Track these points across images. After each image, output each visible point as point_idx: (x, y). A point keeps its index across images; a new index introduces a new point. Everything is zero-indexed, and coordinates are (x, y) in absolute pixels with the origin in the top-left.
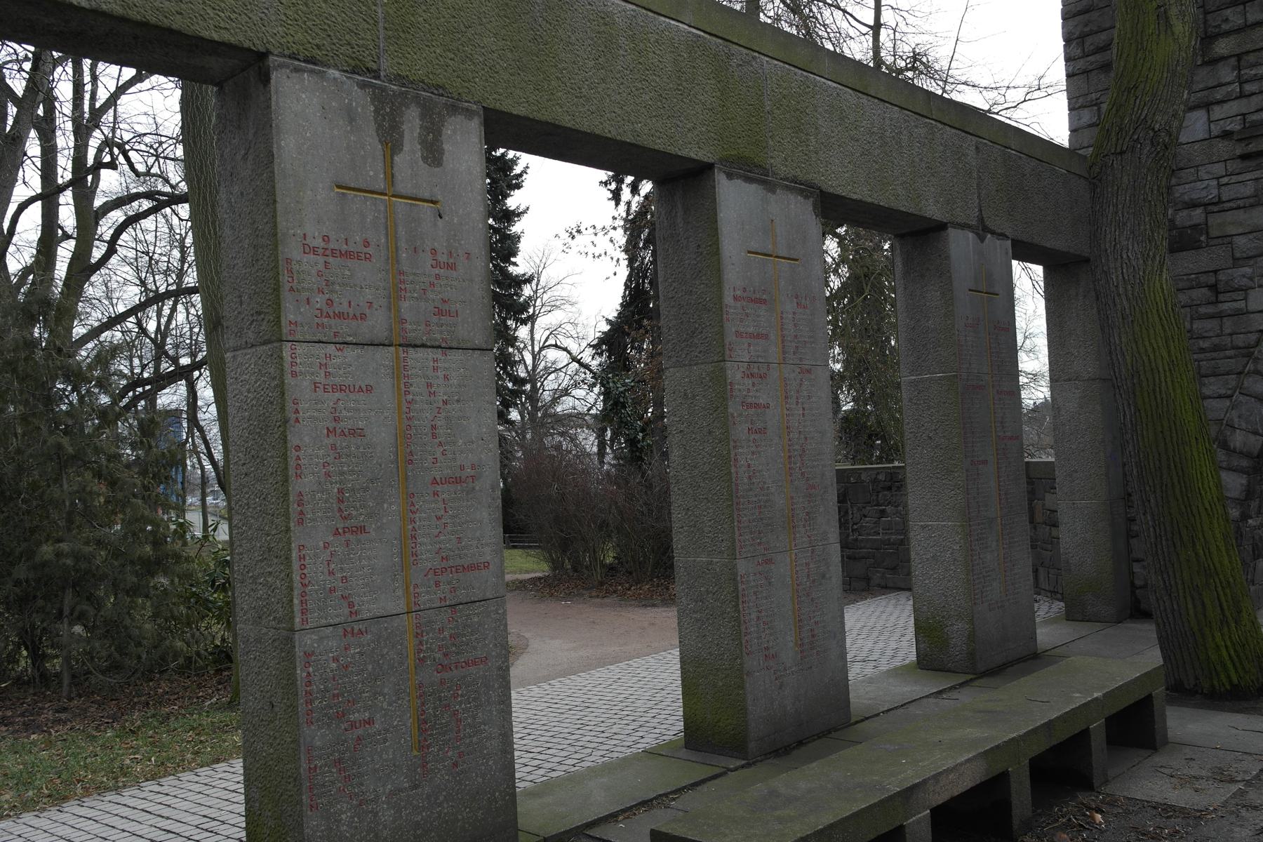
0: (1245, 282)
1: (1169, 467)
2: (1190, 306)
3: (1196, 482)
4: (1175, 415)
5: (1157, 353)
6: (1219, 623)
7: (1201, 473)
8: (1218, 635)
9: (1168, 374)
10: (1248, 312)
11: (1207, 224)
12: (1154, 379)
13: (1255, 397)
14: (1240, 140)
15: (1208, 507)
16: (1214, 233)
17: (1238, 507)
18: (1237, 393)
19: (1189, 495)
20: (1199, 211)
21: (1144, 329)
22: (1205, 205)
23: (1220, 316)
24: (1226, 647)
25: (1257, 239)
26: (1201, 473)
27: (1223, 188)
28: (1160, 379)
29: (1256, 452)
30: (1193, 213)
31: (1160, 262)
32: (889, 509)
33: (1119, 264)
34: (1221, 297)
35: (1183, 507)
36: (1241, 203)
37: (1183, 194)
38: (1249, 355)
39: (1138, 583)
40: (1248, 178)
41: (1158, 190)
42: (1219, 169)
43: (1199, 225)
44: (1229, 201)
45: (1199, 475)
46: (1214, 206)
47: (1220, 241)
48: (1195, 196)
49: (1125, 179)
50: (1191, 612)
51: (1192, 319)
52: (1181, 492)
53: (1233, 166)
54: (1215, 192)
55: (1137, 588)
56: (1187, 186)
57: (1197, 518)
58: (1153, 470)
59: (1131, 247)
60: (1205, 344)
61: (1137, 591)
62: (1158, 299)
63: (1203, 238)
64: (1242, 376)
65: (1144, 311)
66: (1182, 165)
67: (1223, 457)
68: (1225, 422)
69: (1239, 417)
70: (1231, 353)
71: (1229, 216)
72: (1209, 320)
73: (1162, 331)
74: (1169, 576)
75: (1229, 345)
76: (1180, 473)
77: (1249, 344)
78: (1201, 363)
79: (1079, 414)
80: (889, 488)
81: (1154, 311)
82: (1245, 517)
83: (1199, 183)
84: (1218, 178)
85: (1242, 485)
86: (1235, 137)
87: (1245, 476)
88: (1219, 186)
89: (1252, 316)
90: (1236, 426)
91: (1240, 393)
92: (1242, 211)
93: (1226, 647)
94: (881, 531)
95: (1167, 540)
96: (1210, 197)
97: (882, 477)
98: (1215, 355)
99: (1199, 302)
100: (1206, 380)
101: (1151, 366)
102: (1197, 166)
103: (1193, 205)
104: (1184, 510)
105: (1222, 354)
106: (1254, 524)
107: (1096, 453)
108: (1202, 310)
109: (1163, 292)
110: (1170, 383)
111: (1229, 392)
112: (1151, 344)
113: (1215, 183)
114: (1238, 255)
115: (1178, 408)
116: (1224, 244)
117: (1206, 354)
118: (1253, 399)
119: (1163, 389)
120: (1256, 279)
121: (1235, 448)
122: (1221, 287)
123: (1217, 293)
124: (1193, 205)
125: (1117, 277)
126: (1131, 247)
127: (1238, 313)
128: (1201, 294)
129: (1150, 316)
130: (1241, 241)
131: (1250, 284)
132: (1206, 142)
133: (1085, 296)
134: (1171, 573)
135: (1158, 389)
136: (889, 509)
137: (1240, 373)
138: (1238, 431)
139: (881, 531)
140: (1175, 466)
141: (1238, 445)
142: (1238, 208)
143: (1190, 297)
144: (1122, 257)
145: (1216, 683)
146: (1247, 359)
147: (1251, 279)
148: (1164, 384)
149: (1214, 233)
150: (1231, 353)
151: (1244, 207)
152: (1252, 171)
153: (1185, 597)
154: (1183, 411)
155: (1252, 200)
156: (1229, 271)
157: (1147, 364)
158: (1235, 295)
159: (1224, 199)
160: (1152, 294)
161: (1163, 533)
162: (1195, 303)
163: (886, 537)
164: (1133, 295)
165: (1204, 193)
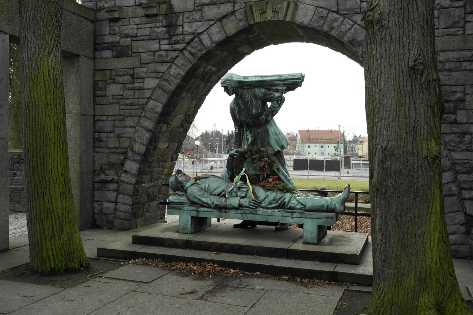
0: (144, 74)
1: (37, 157)
2: (123, 84)
3: (50, 165)
4: (44, 130)
5: (40, 99)
6: (50, 237)
7: (54, 161)
8: (49, 243)
9: (44, 109)
10: (144, 89)
11: (132, 46)
12: (36, 111)
13: (144, 128)
14: (144, 8)
15: (55, 178)
16: (134, 50)
17: (135, 178)
19: (45, 172)
20: (129, 39)
21: (35, 85)
22: (132, 37)
23: (133, 89)
24: (52, 249)
25: (150, 55)
26: (54, 161)
27: (139, 30)
28: (39, 112)
29: (143, 153)
30: (127, 40)
31: (49, 51)
32: (18, 173)
33: (26, 50)
34: (135, 81)
35: (41, 177)
36: (144, 38)
37: (123, 30)
38: (143, 109)
39: (96, 212)
40: (148, 27)
41: (48, 14)
42: (137, 20)
43: (129, 46)
44: (140, 36)
45: (52, 162)
46: (134, 37)
47: (136, 54)
48: (128, 32)
49: (30, 5)
50: (38, 232)
51: (124, 90)
52: (41, 169)
53: (144, 20)
54: (135, 31)
55: (96, 214)
56: (125, 27)
57: (48, 183)
58: (30, 158)
59: (32, 41)
60: (127, 102)
61: (96, 216)
62: (45, 70)
63: (130, 52)
64: (140, 118)
65: (36, 75)
66: (124, 16)
67: (131, 155)
68: (132, 138)
69: (138, 137)
70: (136, 107)
71: (140, 43)
72: (130, 91)
73: (44, 87)
74: (31, 213)
76: (42, 160)
79: (71, 130)
80: (18, 163)
81: (42, 76)
83: (130, 26)
84: (137, 25)
85: (137, 168)
86: (143, 6)
87: (138, 164)
88: (138, 28)
89: (145, 90)
91: (139, 126)
92: (145, 41)
93: (52, 249)
94: (14, 183)
95: (32, 194)
96: (133, 33)
97: (15, 157)
98: (131, 107)
99: (126, 82)
100: (127, 119)
101: (35, 104)
102: (129, 18)
103: (127, 36)
104: (41, 179)
105: (133, 107)
106: (148, 185)
107: (76, 150)
108: (128, 86)
109: (48, 67)
110: (44, 114)
111: (135, 125)
112: (37, 93)
113: (135, 27)
114: (142, 62)
115: (46, 127)
116: (137, 56)
118: (143, 129)
119: (40, 117)
120: (148, 74)
121: (135, 151)
122: (135, 75)
123: (134, 78)
124: (127, 36)
125: (25, 56)
126: (32, 41)
127: (141, 89)
128: (128, 78)
129: (39, 78)
130: (143, 55)
131: (146, 76)
132: (133, 7)
133: (76, 73)
134: (32, 212)
135: (37, 117)
136: (18, 173)
137: (139, 117)
138: (137, 143)
139: (14, 183)
140: (40, 157)
141: (137, 150)
142: (143, 40)
143: (123, 79)
144: (28, 46)
145: (44, 268)
146: (142, 110)
147: (146, 73)
148: (40, 114)
149: (134, 50)
150: (136, 107)
151: (145, 40)
152: (150, 23)
153: (37, 224)
154: (49, 129)
155: (148, 37)
156: (138, 69)
157: (34, 103)
159: (139, 35)
160: (42, 67)
161: (31, 191)
162: (125, 82)
163: (16, 187)
164: (31, 66)
165: (131, 31)
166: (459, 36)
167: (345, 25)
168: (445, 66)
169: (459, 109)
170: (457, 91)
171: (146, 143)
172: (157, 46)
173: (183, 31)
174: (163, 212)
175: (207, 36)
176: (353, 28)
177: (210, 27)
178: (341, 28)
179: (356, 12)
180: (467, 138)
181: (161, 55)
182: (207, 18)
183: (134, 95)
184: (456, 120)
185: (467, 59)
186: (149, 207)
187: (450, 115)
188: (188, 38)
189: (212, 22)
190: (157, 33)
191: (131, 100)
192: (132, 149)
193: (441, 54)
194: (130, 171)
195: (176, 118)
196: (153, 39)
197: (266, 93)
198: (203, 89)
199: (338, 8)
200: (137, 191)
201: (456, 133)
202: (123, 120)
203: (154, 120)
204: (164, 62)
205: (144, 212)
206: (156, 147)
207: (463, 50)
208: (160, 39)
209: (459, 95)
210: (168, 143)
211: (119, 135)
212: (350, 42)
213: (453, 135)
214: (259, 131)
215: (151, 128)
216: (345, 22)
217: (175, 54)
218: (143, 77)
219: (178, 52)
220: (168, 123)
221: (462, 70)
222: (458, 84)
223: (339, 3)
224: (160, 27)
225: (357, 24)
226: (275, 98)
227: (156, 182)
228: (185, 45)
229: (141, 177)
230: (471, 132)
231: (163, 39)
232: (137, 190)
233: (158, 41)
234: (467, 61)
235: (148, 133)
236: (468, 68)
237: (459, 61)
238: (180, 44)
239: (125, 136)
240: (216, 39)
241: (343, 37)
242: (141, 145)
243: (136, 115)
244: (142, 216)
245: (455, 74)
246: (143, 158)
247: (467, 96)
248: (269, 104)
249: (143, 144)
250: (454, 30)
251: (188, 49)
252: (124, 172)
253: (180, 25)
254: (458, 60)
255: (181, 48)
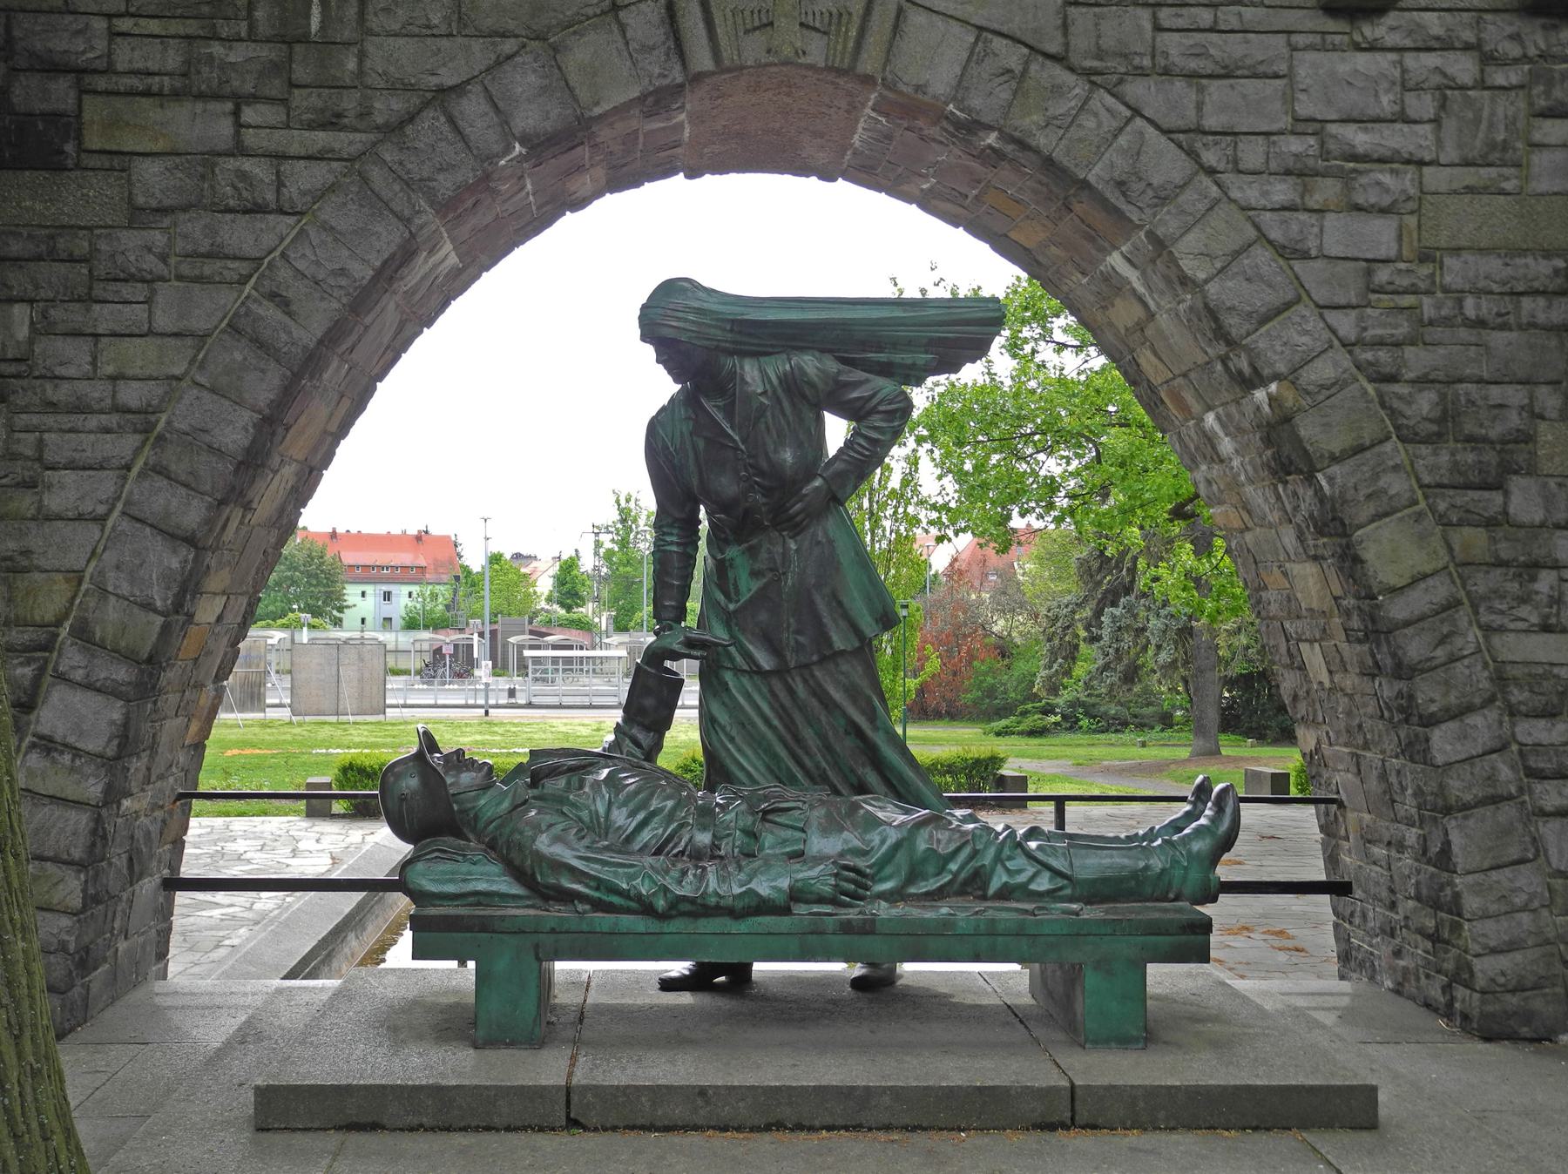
0: (151, 263)
13: (151, 526)
16: (94, 141)
18: (116, 513)
27: (119, 40)
38: (147, 429)
43: (62, 115)
47: (105, 161)
63: (69, 148)
75: (109, 401)
77: (150, 405)
78: (46, 436)
82: (113, 795)
83: (71, 18)
84: (109, 16)
85: (112, 722)
88: (114, 34)
90: (110, 589)
96: (91, 55)
111: (101, 509)
113: (100, 24)
116: (112, 169)
117: (59, 417)
120: (173, 261)
121: (103, 639)
131: (160, 268)
138: (111, 597)
142: (147, 93)
146: (138, 438)
147: (164, 258)
151: (160, 94)
158: (126, 291)
159: (120, 67)
162: (43, 294)
166: (1509, 198)
167: (1096, 115)
168: (1461, 307)
169: (1516, 472)
170: (1506, 403)
171: (165, 600)
172: (225, 128)
173: (361, 73)
174: (165, 925)
175: (485, 107)
176: (1128, 129)
177: (499, 63)
178: (1080, 126)
179: (1136, 68)
180: (1545, 582)
181: (243, 175)
182: (488, 23)
183: (95, 359)
184: (1505, 513)
185: (1536, 284)
186: (131, 907)
187: (1486, 494)
188: (387, 107)
189: (509, 46)
190: (225, 66)
191: (83, 387)
192: (82, 633)
193: (1448, 261)
194: (71, 740)
195: (278, 477)
196: (200, 96)
197: (843, 378)
198: (384, 353)
199: (1067, 45)
200: (104, 837)
201: (1501, 563)
202: (30, 484)
203: (208, 487)
204: (258, 209)
205: (112, 935)
206: (190, 616)
207: (1523, 252)
208: (240, 101)
209: (1514, 420)
210: (225, 598)
211: (10, 558)
212: (1120, 184)
213: (1499, 571)
214: (793, 546)
215: (195, 526)
216: (1095, 104)
217: (319, 174)
218: (149, 277)
219: (335, 165)
220: (251, 501)
221: (1520, 327)
222: (1507, 379)
223: (1069, 21)
224: (241, 40)
225: (1143, 116)
226: (879, 404)
227: (159, 784)
228: (372, 137)
229: (124, 767)
230: (1557, 560)
231: (254, 99)
232: (104, 829)
233: (229, 106)
234: (1535, 293)
235: (175, 551)
236: (1541, 318)
237: (1512, 293)
238: (343, 128)
239: (42, 563)
240: (530, 121)
241: (1090, 165)
242: (136, 610)
243: (106, 459)
244: (105, 960)
245: (1498, 339)
246: (142, 672)
247: (1543, 426)
248: (836, 431)
249: (148, 606)
250: (1493, 172)
251: (388, 158)
252: (33, 746)
253: (347, 44)
254: (1506, 289)
255: (353, 150)
